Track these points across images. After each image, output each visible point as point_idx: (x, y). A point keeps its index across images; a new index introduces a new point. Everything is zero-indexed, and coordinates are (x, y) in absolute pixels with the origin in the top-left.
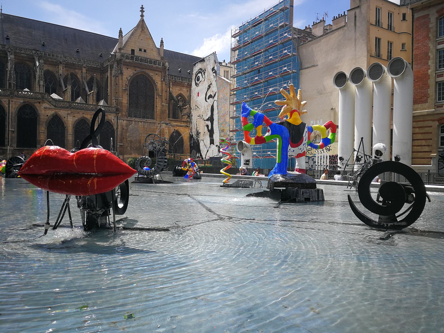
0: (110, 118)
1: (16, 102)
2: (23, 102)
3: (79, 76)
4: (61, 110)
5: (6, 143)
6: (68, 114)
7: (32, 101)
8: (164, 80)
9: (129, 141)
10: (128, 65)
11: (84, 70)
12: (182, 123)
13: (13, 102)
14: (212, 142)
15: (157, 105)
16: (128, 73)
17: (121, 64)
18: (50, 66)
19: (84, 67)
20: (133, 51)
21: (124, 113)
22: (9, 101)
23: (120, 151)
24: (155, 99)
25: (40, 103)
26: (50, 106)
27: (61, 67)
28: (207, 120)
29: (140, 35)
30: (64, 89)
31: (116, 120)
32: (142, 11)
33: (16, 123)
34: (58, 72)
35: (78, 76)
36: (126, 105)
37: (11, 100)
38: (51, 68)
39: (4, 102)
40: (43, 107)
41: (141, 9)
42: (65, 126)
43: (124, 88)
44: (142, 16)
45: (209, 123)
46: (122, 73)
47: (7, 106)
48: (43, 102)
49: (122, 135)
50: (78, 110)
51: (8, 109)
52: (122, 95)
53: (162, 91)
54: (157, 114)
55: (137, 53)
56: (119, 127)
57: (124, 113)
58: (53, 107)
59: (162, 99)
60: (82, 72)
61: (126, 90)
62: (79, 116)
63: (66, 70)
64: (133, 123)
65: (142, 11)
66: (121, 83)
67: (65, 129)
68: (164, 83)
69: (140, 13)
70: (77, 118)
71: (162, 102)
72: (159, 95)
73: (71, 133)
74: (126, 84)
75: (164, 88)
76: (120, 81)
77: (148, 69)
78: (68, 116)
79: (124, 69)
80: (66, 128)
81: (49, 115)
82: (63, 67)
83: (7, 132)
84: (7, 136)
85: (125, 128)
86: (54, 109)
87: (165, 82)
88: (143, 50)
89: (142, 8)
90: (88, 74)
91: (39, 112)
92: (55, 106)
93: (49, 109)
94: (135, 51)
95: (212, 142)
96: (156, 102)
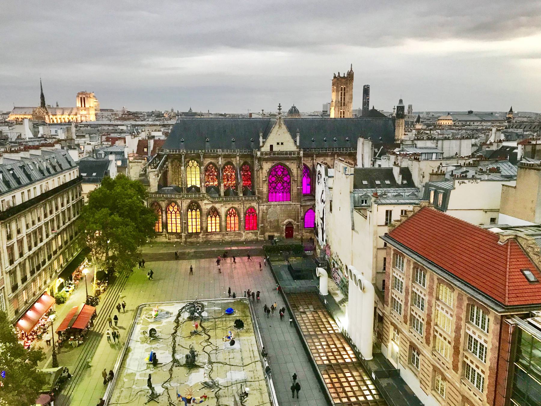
3: (234, 163)
8: (299, 167)
10: (267, 160)
11: (238, 158)
16: (267, 166)
17: (261, 160)
19: (238, 156)
20: (271, 146)
21: (264, 200)
25: (201, 200)
27: (220, 159)
29: (278, 131)
34: (218, 163)
35: (234, 163)
38: (213, 161)
43: (264, 180)
46: (262, 168)
47: (181, 205)
48: (204, 200)
49: (262, 217)
53: (298, 176)
55: (275, 149)
57: (264, 200)
61: (265, 180)
63: (225, 160)
66: (261, 176)
68: (299, 169)
72: (294, 180)
75: (299, 174)
76: (261, 174)
85: (265, 211)
88: (280, 144)
89: (280, 106)
92: (212, 202)
93: (208, 204)
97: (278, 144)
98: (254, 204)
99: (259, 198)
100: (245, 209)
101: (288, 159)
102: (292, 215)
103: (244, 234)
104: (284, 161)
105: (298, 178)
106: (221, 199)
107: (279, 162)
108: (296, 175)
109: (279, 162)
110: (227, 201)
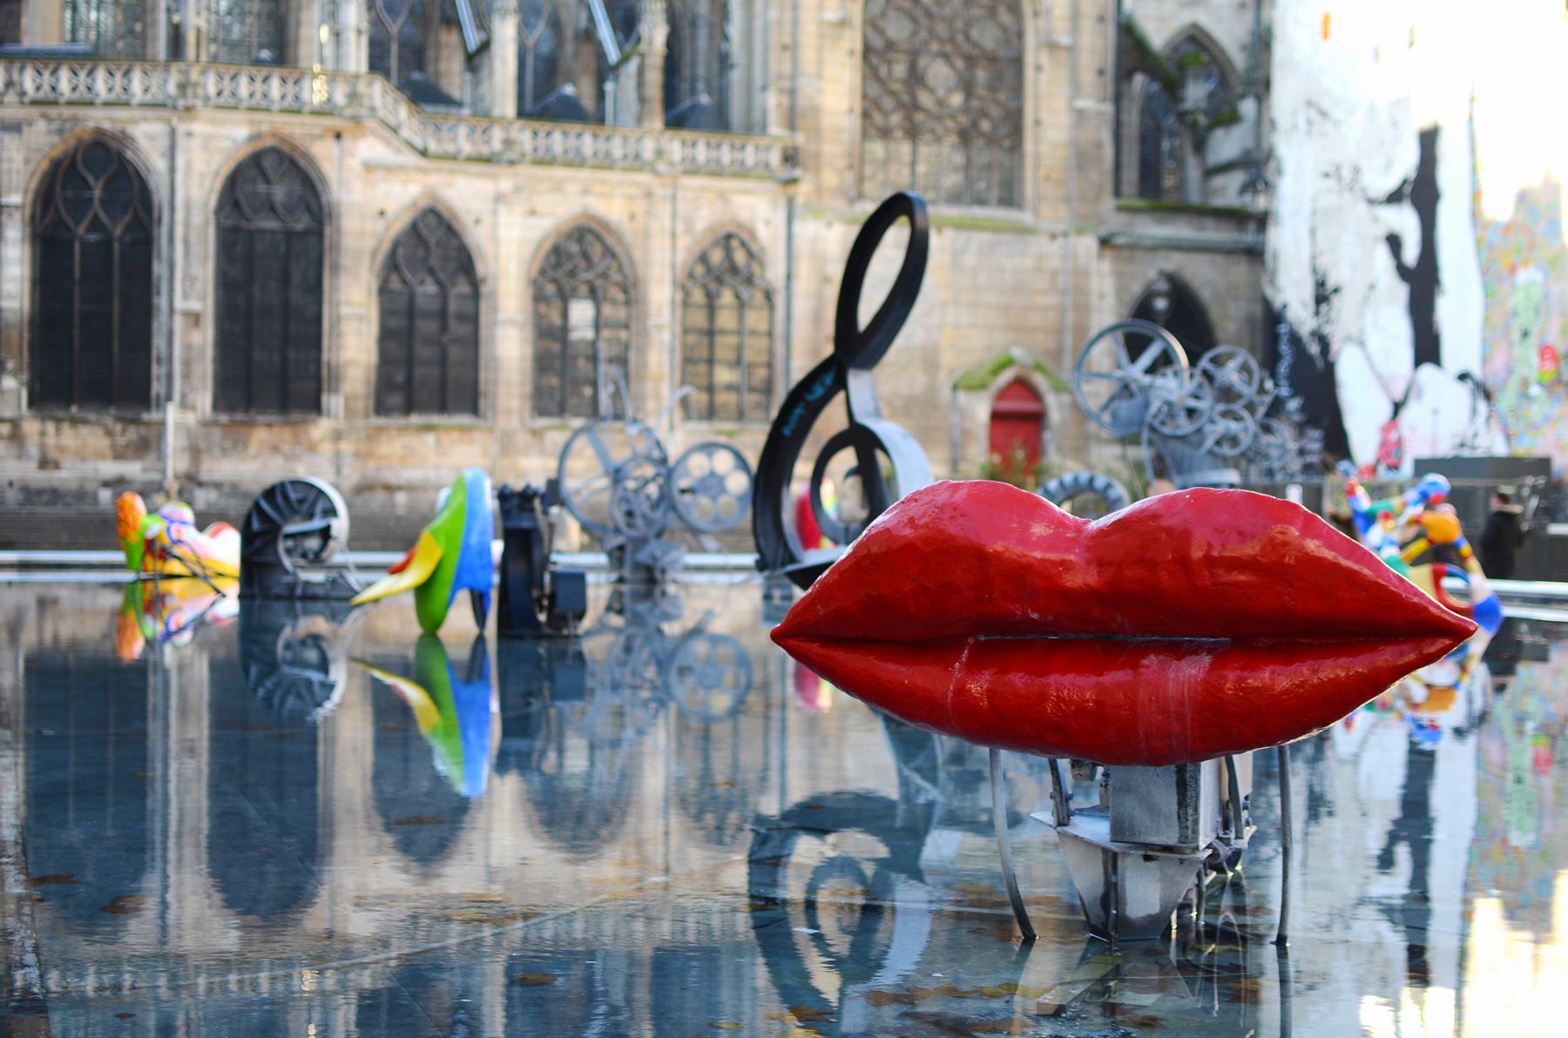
0: (744, 216)
1: (208, 139)
5: (157, 388)
6: (499, 198)
12: (1210, 223)
14: (1427, 348)
22: (173, 134)
25: (338, 136)
26: (398, 151)
28: (1394, 198)
30: (473, 39)
37: (182, 128)
39: (143, 143)
45: (1406, 221)
50: (559, 172)
56: (803, 269)
58: (412, 159)
59: (1074, 69)
61: (843, 23)
71: (1076, 88)
72: (1052, 46)
84: (159, 342)
86: (419, 169)
93: (389, 169)
95: (1427, 348)
96: (1037, 98)
99: (790, 158)
100: (684, 242)
102: (1035, 319)
106: (497, 135)
110: (544, 160)
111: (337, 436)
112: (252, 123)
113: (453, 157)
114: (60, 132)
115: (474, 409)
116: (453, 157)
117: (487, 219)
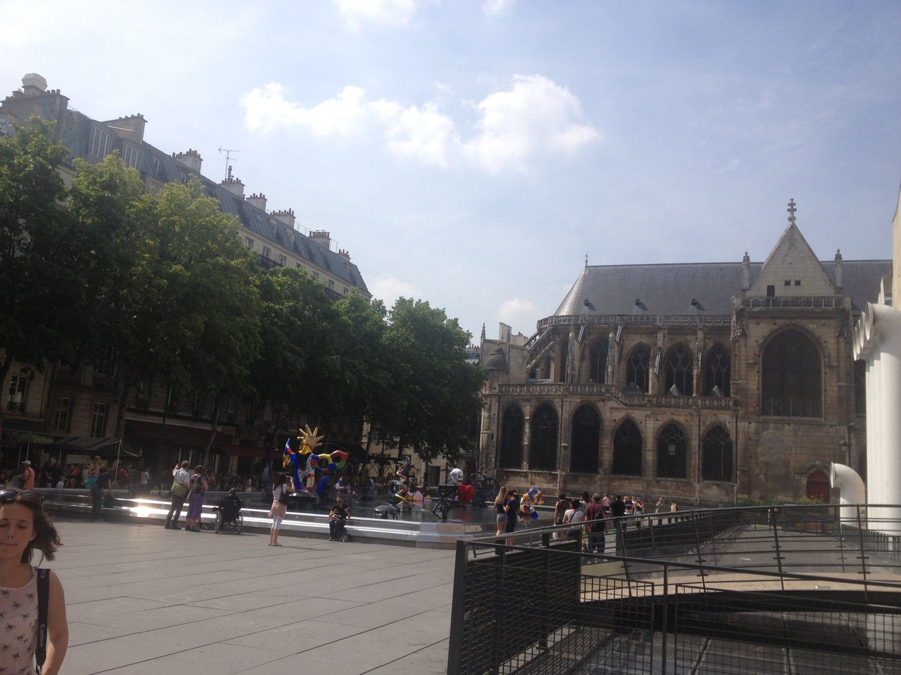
0: (722, 420)
1: (570, 402)
2: (581, 402)
4: (636, 409)
6: (647, 416)
7: (593, 399)
9: (762, 462)
10: (758, 318)
11: (700, 335)
13: (568, 403)
15: (827, 388)
16: (759, 332)
18: (644, 336)
19: (701, 329)
20: (771, 289)
22: (562, 401)
23: (742, 483)
24: (823, 375)
25: (603, 401)
26: (619, 404)
27: (660, 336)
31: (734, 423)
32: (792, 210)
33: (570, 434)
34: (655, 344)
36: (756, 392)
37: (565, 400)
38: (645, 340)
40: (608, 408)
41: (790, 207)
42: (642, 435)
44: (792, 219)
46: (744, 335)
47: (560, 410)
48: (609, 399)
50: (664, 409)
51: (561, 412)
52: (747, 375)
53: (838, 357)
54: (827, 406)
55: (779, 292)
56: (741, 436)
58: (622, 406)
60: (697, 338)
61: (755, 364)
62: (664, 418)
64: (771, 427)
65: (792, 210)
66: (743, 353)
67: (641, 443)
68: (841, 339)
69: (789, 214)
70: (661, 423)
72: (831, 367)
73: (652, 449)
74: (755, 354)
76: (743, 349)
77: (804, 318)
78: (646, 420)
79: (750, 325)
80: (644, 441)
81: (617, 419)
82: (664, 334)
83: (559, 447)
85: (753, 436)
86: (626, 409)
87: (845, 338)
88: (793, 283)
89: (792, 204)
90: (709, 339)
91: (603, 415)
92: (626, 404)
93: (617, 409)
94: (775, 288)
97: (787, 283)
98: (726, 418)
99: (736, 403)
100: (702, 428)
101: (812, 316)
103: (697, 486)
104: (806, 321)
105: (838, 361)
106: (646, 399)
107: (789, 321)
108: (833, 354)
109: (789, 321)
111: (602, 480)
112: (581, 398)
113: (634, 406)
114: (538, 401)
115: (640, 475)
116: (634, 406)
117: (643, 422)
